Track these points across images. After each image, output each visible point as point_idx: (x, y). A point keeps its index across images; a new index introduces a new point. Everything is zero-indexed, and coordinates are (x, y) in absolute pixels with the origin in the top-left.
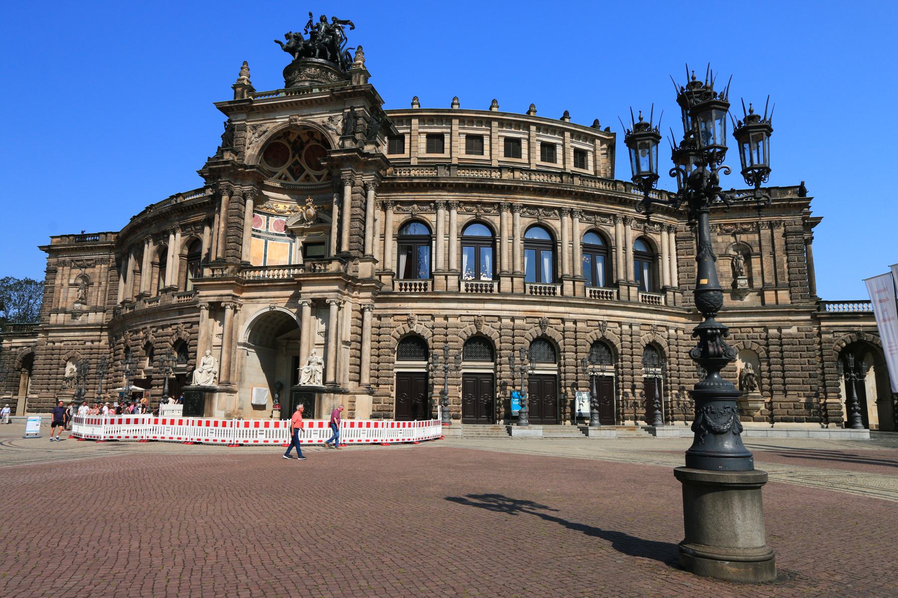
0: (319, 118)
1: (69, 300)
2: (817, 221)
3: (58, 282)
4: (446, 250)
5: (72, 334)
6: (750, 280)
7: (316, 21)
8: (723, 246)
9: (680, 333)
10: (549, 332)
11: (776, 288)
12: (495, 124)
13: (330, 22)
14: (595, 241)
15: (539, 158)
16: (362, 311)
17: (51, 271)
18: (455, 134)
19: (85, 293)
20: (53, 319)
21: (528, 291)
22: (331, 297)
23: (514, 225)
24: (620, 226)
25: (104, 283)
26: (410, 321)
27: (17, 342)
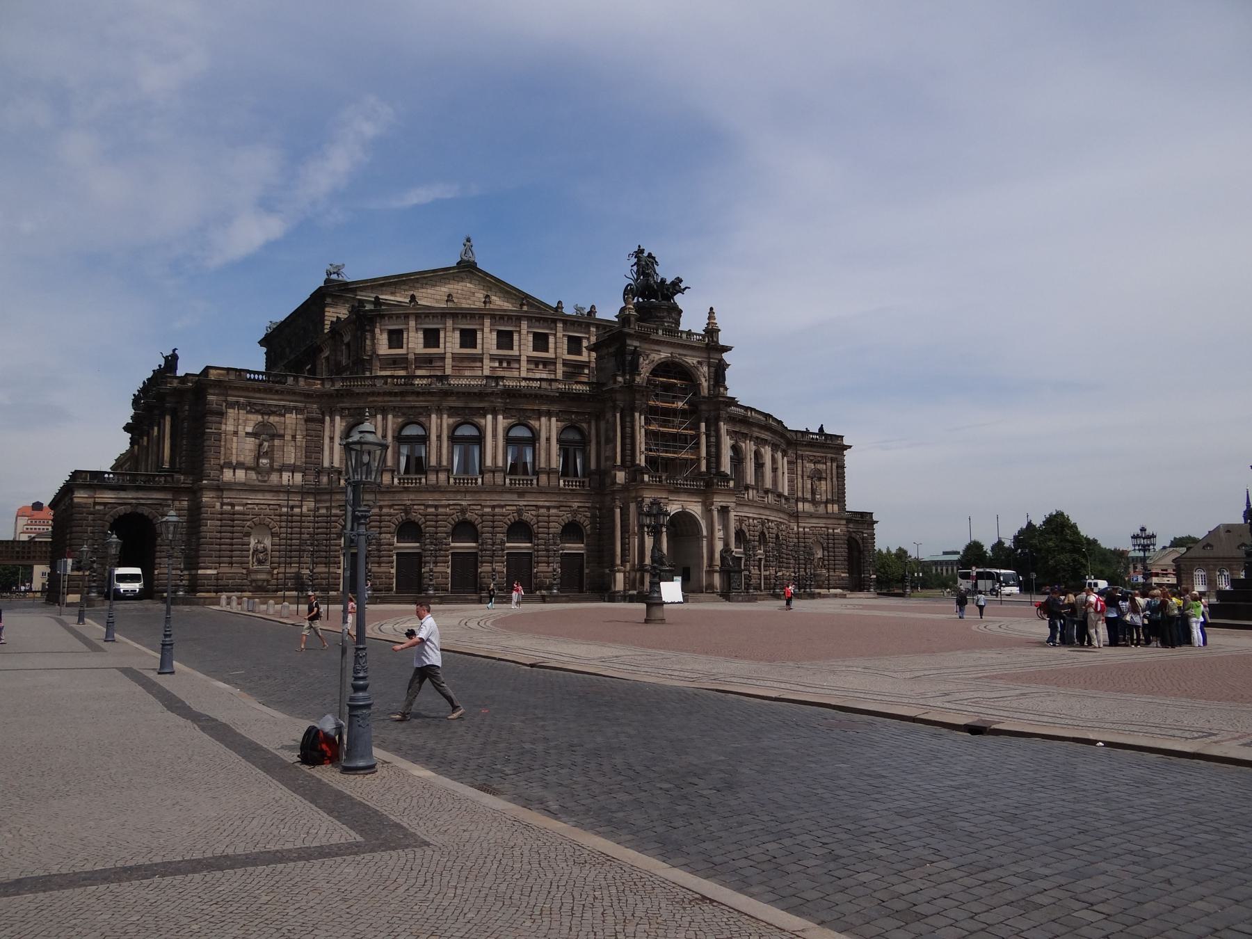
0: (691, 360)
3: (230, 427)
11: (833, 502)
13: (646, 254)
20: (228, 475)
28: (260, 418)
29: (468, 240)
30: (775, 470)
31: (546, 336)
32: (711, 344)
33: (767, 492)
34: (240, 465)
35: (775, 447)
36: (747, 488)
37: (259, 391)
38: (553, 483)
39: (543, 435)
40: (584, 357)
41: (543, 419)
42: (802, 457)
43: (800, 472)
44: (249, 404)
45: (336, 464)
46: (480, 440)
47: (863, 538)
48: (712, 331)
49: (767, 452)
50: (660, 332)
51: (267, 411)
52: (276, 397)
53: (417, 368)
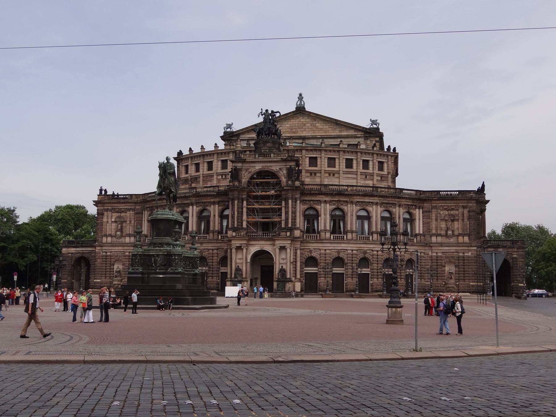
1: (113, 230)
2: (488, 201)
3: (105, 220)
4: (324, 222)
5: (117, 248)
6: (453, 231)
7: (264, 111)
8: (443, 215)
9: (422, 254)
10: (367, 256)
11: (463, 235)
12: (341, 153)
13: (270, 112)
14: (386, 215)
15: (361, 168)
16: (296, 250)
17: (100, 213)
18: (323, 158)
19: (122, 227)
20: (104, 240)
21: (358, 238)
22: (288, 246)
23: (353, 210)
24: (397, 208)
25: (133, 222)
26: (311, 251)
27: (73, 250)
28: (117, 214)
29: (300, 95)
34: (111, 236)
37: (115, 203)
38: (216, 237)
43: (434, 218)
45: (145, 233)
47: (513, 258)
50: (257, 156)
51: (120, 211)
52: (123, 205)
53: (192, 183)
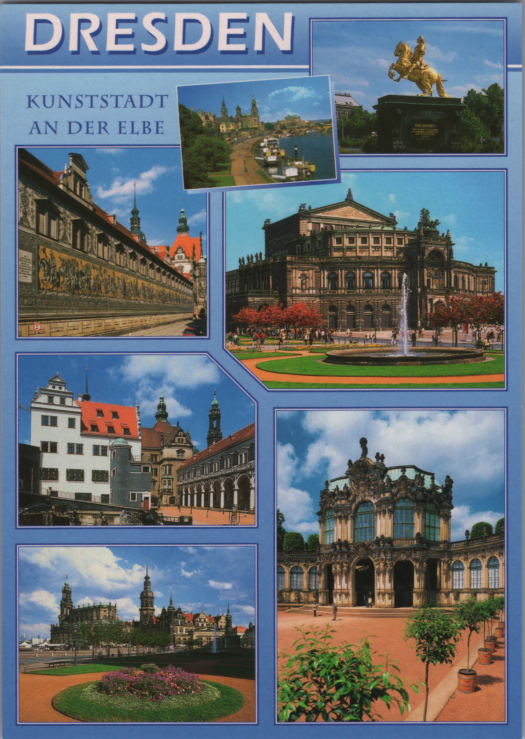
3: (294, 276)
11: (490, 292)
20: (294, 291)
30: (469, 282)
31: (390, 239)
32: (448, 242)
33: (466, 291)
35: (469, 274)
36: (459, 290)
39: (393, 275)
40: (403, 246)
41: (393, 271)
42: (479, 276)
44: (299, 268)
46: (372, 278)
48: (448, 238)
49: (466, 277)
51: (303, 270)
